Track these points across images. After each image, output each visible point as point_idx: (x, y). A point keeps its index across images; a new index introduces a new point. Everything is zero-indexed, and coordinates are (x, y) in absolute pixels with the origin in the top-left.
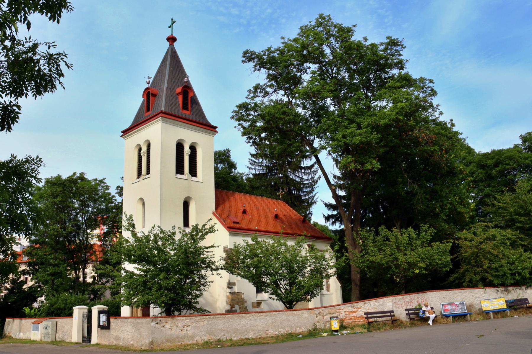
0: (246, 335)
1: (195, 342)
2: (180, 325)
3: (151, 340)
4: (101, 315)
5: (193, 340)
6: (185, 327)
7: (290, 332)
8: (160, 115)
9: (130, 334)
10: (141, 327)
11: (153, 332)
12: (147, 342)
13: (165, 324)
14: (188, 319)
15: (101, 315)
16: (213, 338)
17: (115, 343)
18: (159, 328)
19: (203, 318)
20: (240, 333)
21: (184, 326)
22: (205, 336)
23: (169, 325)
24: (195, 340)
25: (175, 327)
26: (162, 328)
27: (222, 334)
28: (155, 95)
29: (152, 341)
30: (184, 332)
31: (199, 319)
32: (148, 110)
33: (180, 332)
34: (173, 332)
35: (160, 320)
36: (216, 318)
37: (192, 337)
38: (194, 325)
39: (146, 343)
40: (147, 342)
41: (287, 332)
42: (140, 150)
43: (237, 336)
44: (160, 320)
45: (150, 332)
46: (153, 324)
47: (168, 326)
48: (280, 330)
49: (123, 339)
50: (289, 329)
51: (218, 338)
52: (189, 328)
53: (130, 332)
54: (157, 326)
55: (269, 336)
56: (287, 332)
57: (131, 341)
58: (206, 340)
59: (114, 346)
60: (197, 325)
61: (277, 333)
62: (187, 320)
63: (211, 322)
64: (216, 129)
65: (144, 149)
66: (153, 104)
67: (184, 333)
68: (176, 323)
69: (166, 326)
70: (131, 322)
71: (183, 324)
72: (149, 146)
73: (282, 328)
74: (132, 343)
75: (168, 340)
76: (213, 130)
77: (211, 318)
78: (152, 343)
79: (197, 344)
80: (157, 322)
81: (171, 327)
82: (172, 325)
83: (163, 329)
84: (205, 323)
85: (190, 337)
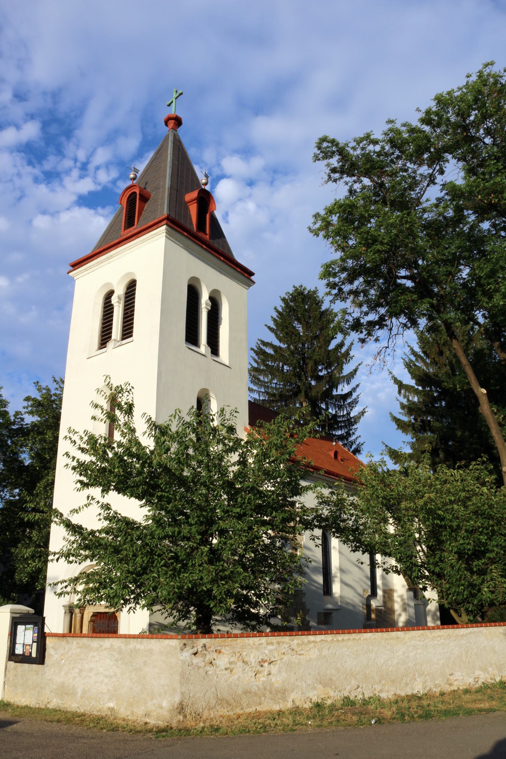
0: (407, 684)
1: (290, 705)
2: (253, 658)
3: (177, 699)
4: (21, 628)
5: (285, 699)
6: (266, 664)
7: (498, 679)
8: (165, 222)
9: (106, 680)
10: (145, 663)
11: (184, 678)
12: (165, 704)
13: (215, 655)
14: (272, 644)
15: (21, 628)
16: (332, 694)
17: (55, 703)
18: (199, 668)
19: (309, 642)
20: (393, 682)
21: (261, 663)
22: (314, 688)
23: (226, 660)
24: (290, 700)
25: (240, 664)
26: (208, 668)
27: (354, 683)
28: (145, 199)
29: (181, 704)
30: (263, 679)
31: (298, 645)
32: (130, 222)
33: (253, 679)
34: (236, 677)
35: (205, 646)
36: (338, 641)
37: (282, 693)
38: (286, 658)
39: (161, 707)
40: (165, 704)
41: (491, 679)
42: (110, 294)
43: (386, 688)
44: (205, 646)
45: (177, 678)
46: (187, 654)
47: (222, 661)
48: (477, 673)
49: (84, 692)
50: (496, 672)
51: (346, 695)
52: (274, 669)
53: (106, 677)
54: (196, 660)
55: (456, 688)
56: (491, 679)
57: (110, 699)
58: (315, 699)
59: (55, 710)
60: (295, 659)
61: (471, 680)
62: (270, 647)
63: (325, 652)
64: (253, 278)
65: (120, 291)
66: (140, 214)
67: (263, 681)
68: (244, 654)
69: (217, 662)
70: (112, 647)
71: (261, 657)
72: (131, 286)
73: (481, 669)
74: (111, 705)
75: (221, 701)
76: (249, 277)
77: (326, 641)
78: (181, 709)
79: (296, 711)
80: (195, 650)
81: (231, 663)
82: (232, 659)
83: (211, 670)
84: (314, 653)
85: (277, 692)
